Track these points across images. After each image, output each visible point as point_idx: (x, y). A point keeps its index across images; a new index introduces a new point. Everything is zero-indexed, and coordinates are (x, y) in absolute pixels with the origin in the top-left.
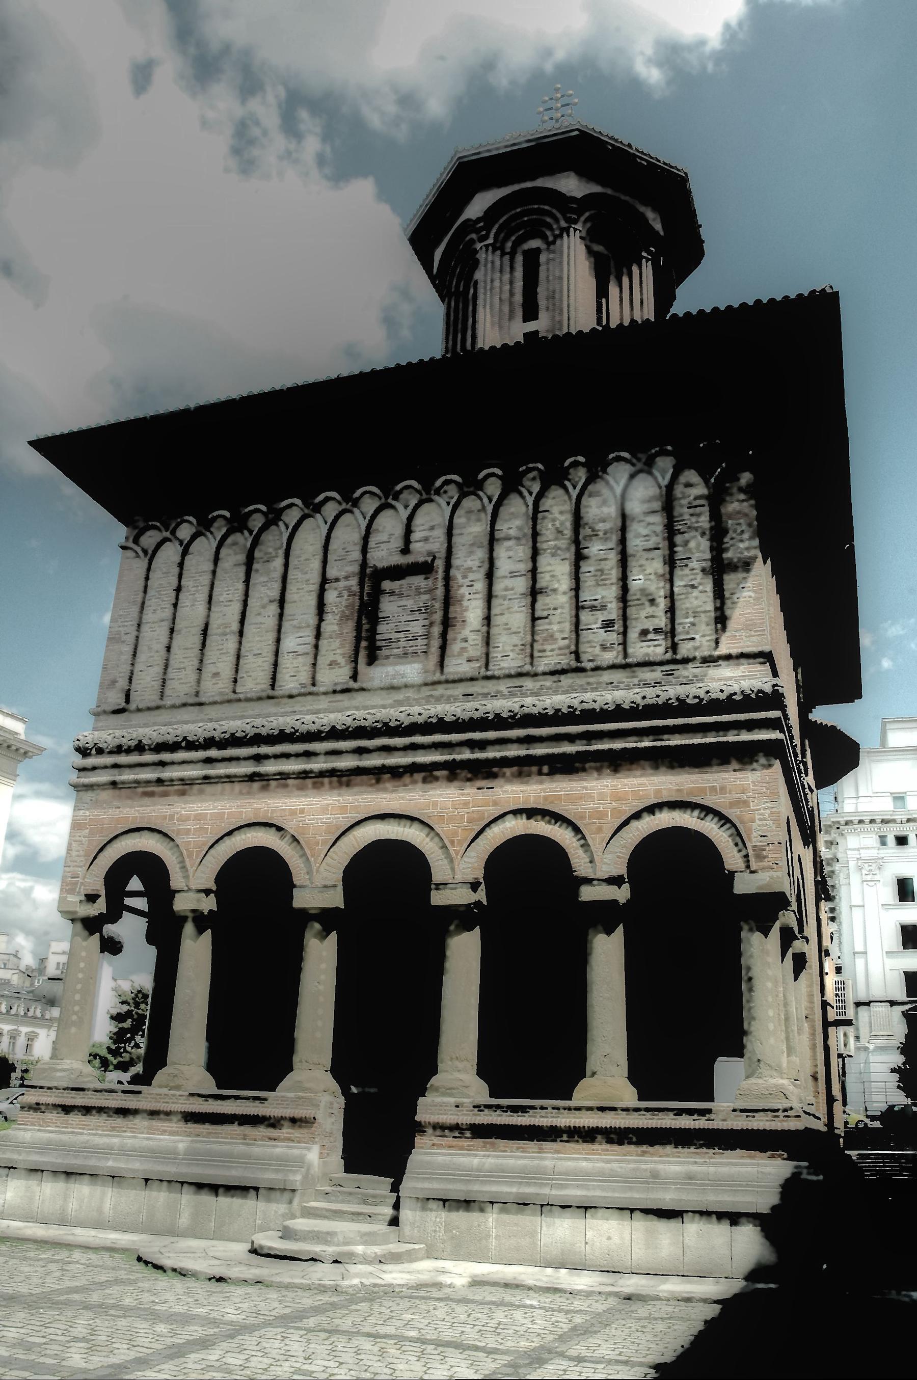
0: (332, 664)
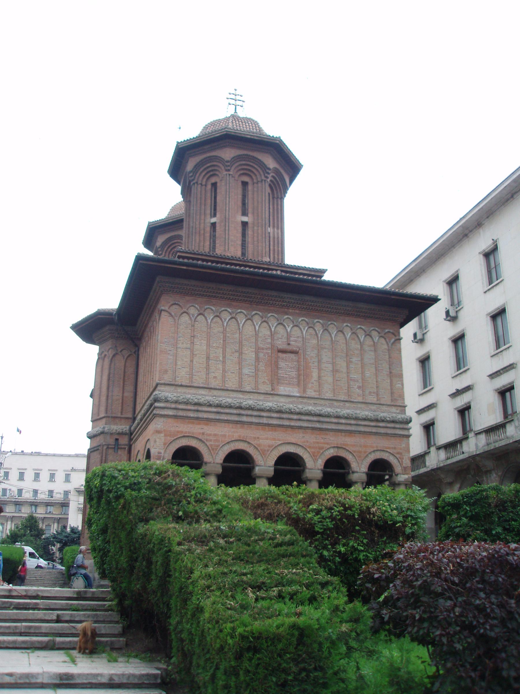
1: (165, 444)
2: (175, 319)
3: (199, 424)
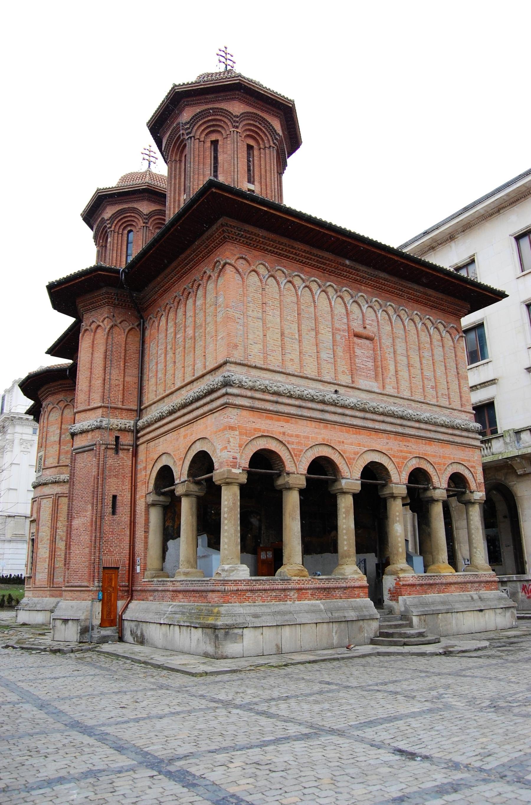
0: (343, 372)
1: (240, 446)
2: (242, 278)
3: (279, 420)
